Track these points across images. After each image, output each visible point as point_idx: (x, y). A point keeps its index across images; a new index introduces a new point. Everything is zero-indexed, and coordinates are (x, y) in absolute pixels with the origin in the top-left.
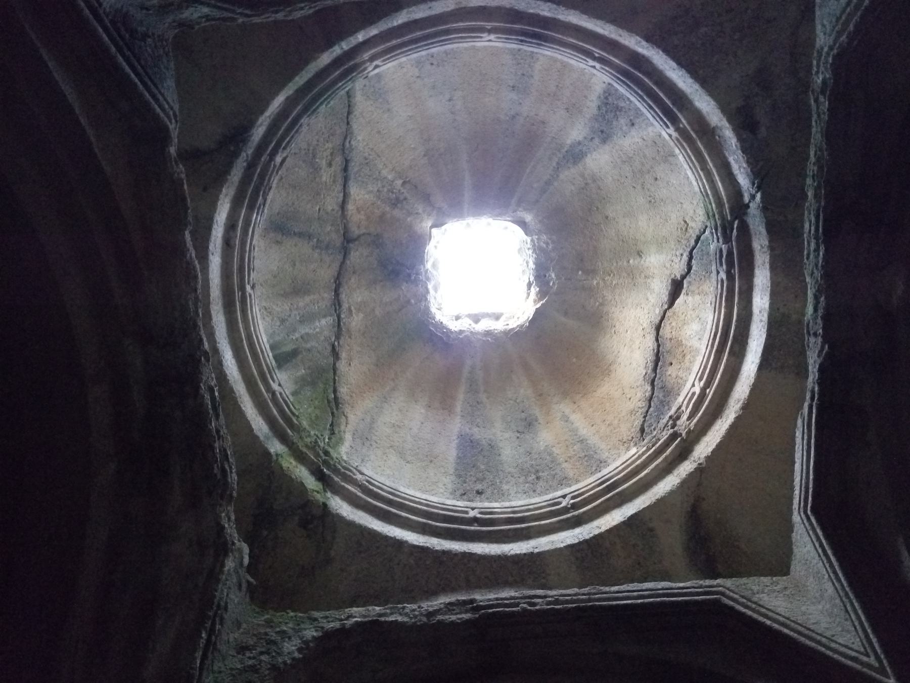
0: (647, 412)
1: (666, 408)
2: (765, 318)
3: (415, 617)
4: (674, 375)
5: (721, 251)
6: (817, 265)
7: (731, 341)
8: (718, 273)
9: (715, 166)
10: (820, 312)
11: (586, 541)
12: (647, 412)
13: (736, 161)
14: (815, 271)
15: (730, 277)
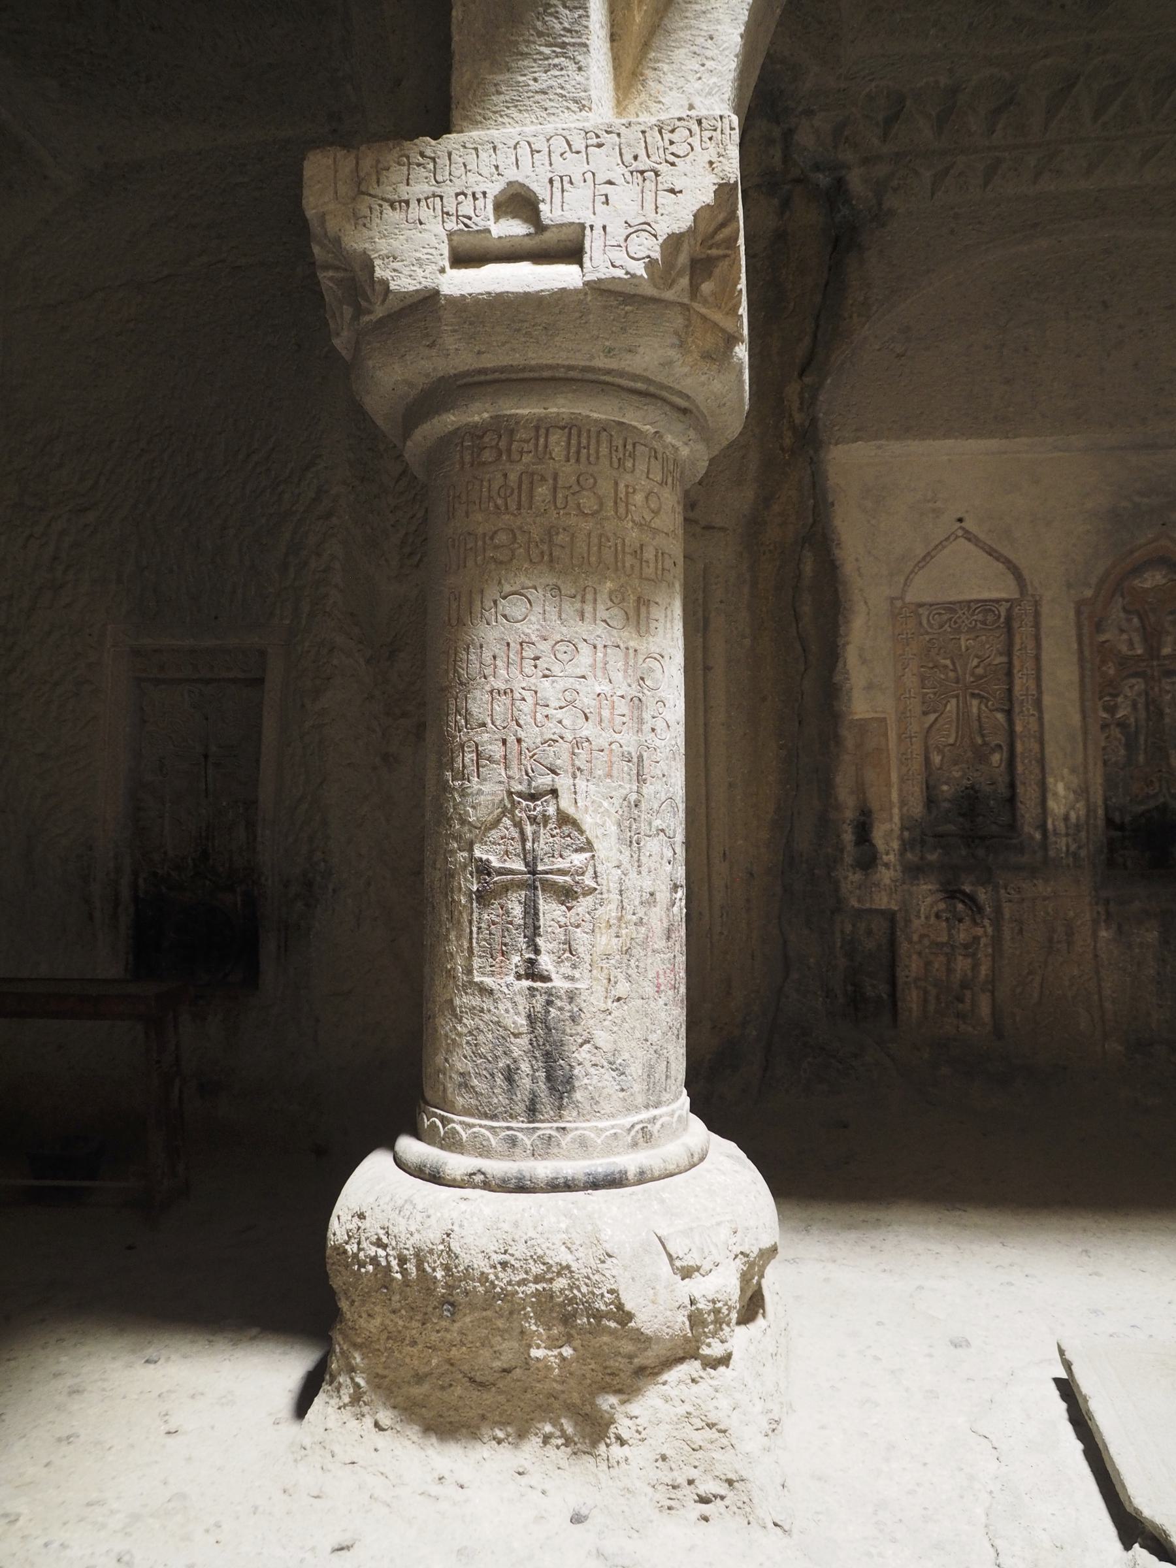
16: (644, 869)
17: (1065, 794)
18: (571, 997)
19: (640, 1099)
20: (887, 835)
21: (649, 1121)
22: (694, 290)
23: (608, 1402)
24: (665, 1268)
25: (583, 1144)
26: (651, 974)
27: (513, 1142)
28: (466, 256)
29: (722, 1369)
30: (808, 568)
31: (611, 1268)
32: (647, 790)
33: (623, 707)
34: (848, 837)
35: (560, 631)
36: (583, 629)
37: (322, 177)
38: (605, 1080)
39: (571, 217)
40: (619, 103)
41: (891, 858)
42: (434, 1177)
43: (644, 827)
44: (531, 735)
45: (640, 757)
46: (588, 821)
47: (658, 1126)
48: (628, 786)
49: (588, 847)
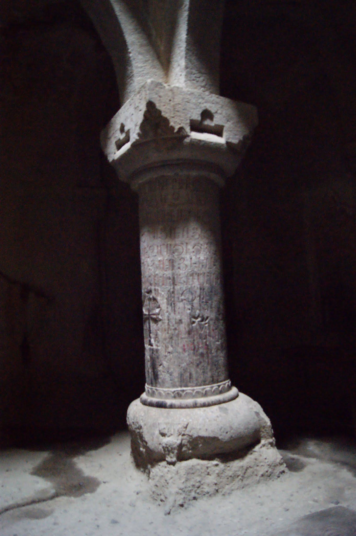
16: (177, 313)
18: (157, 351)
19: (178, 384)
21: (181, 391)
24: (157, 432)
25: (160, 394)
26: (181, 345)
29: (172, 466)
32: (177, 287)
33: (167, 263)
35: (151, 243)
43: (176, 299)
45: (174, 278)
46: (159, 298)
47: (185, 393)
48: (169, 287)
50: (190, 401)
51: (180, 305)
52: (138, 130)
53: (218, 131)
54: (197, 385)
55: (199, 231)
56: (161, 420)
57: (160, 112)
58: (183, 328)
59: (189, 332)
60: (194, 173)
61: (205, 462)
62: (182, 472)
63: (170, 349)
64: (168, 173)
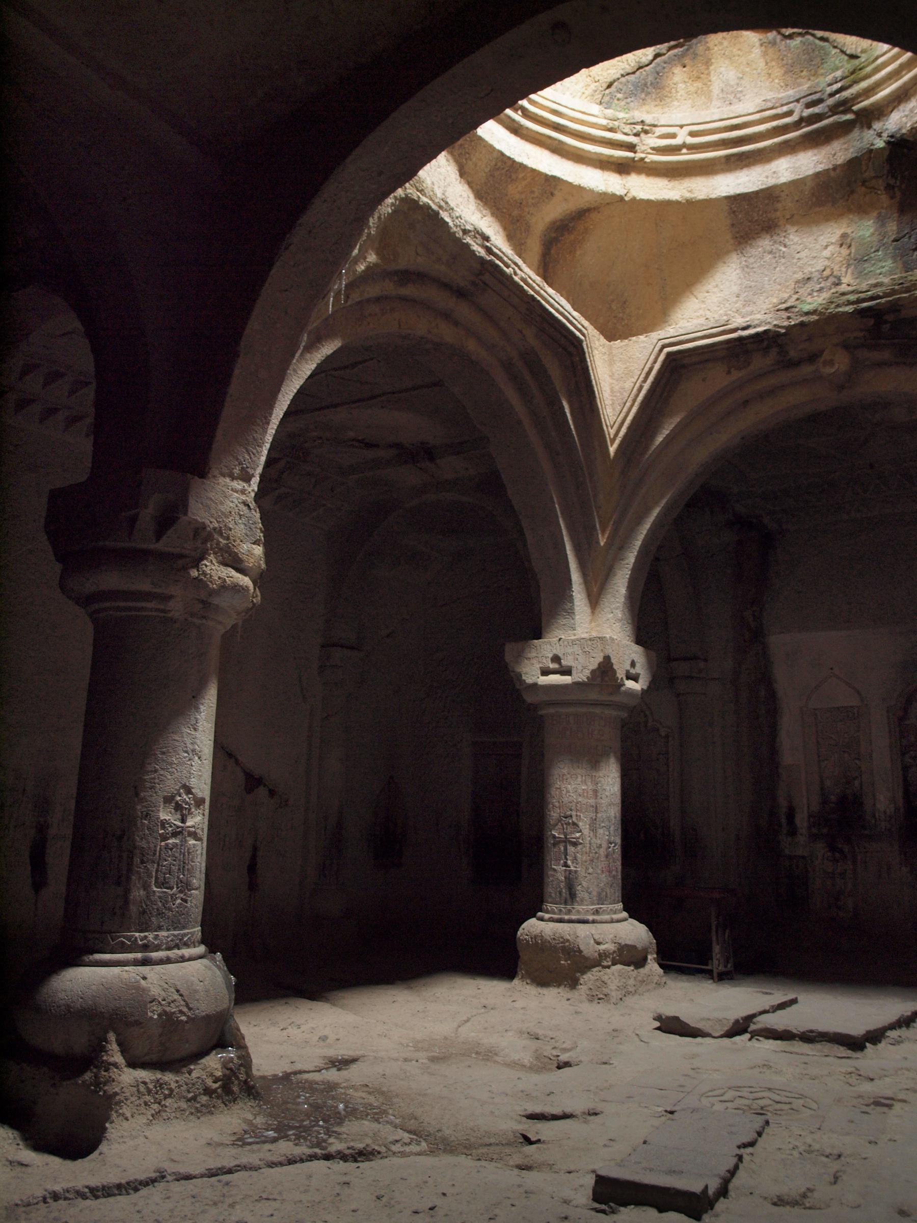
0: (628, 74)
1: (643, 96)
2: (771, 182)
3: (456, 226)
4: (676, 79)
5: (820, 101)
6: (838, 306)
7: (739, 152)
8: (798, 101)
9: (905, 84)
10: (804, 319)
11: (514, 161)
12: (628, 74)
13: (911, 111)
14: (833, 306)
15: (797, 125)
17: (883, 800)
18: (576, 872)
20: (801, 820)
22: (602, 680)
23: (578, 975)
24: (592, 941)
25: (578, 912)
27: (561, 910)
28: (545, 672)
30: (763, 693)
31: (578, 940)
32: (599, 815)
34: (784, 821)
36: (579, 771)
37: (509, 649)
38: (586, 896)
39: (569, 664)
40: (593, 613)
41: (804, 831)
42: (541, 919)
44: (565, 800)
46: (580, 824)
49: (580, 831)
50: (606, 917)
51: (601, 831)
52: (587, 673)
53: (635, 678)
54: (611, 904)
55: (614, 766)
56: (593, 932)
57: (612, 664)
58: (602, 852)
59: (607, 856)
60: (614, 713)
61: (626, 967)
62: (616, 974)
63: (591, 870)
64: (598, 710)
